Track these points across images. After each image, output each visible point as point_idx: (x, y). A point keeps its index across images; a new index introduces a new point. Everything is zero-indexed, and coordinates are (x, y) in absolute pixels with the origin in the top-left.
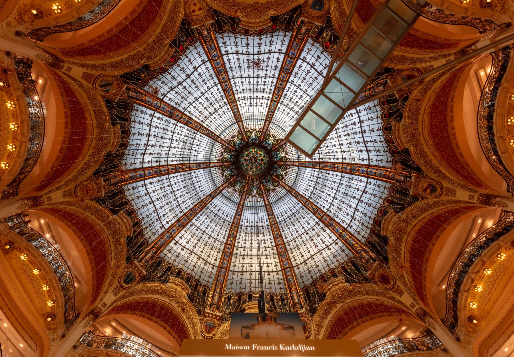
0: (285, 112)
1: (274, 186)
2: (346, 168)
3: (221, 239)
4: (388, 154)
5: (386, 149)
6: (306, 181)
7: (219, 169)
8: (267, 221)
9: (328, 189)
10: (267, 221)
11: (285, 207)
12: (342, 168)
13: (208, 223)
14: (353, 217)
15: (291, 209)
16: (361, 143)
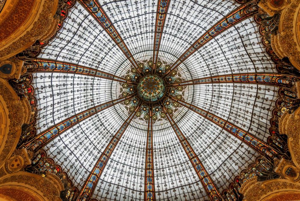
0: (170, 40)
1: (176, 107)
2: (236, 79)
3: (141, 166)
4: (271, 62)
5: (269, 58)
6: (202, 95)
7: (122, 104)
8: (176, 140)
9: (224, 99)
10: (176, 140)
11: (190, 123)
12: (232, 79)
13: (125, 155)
14: (251, 121)
15: (195, 123)
16: (245, 56)
